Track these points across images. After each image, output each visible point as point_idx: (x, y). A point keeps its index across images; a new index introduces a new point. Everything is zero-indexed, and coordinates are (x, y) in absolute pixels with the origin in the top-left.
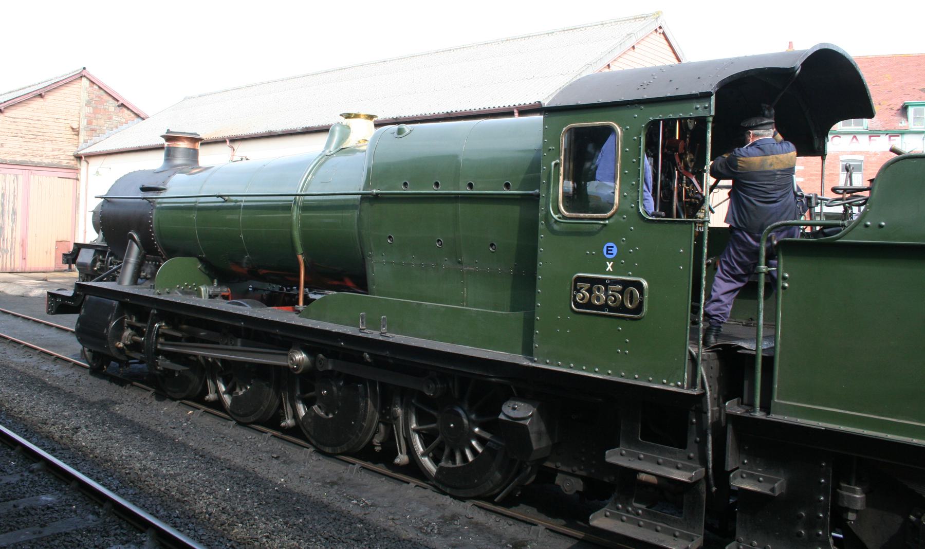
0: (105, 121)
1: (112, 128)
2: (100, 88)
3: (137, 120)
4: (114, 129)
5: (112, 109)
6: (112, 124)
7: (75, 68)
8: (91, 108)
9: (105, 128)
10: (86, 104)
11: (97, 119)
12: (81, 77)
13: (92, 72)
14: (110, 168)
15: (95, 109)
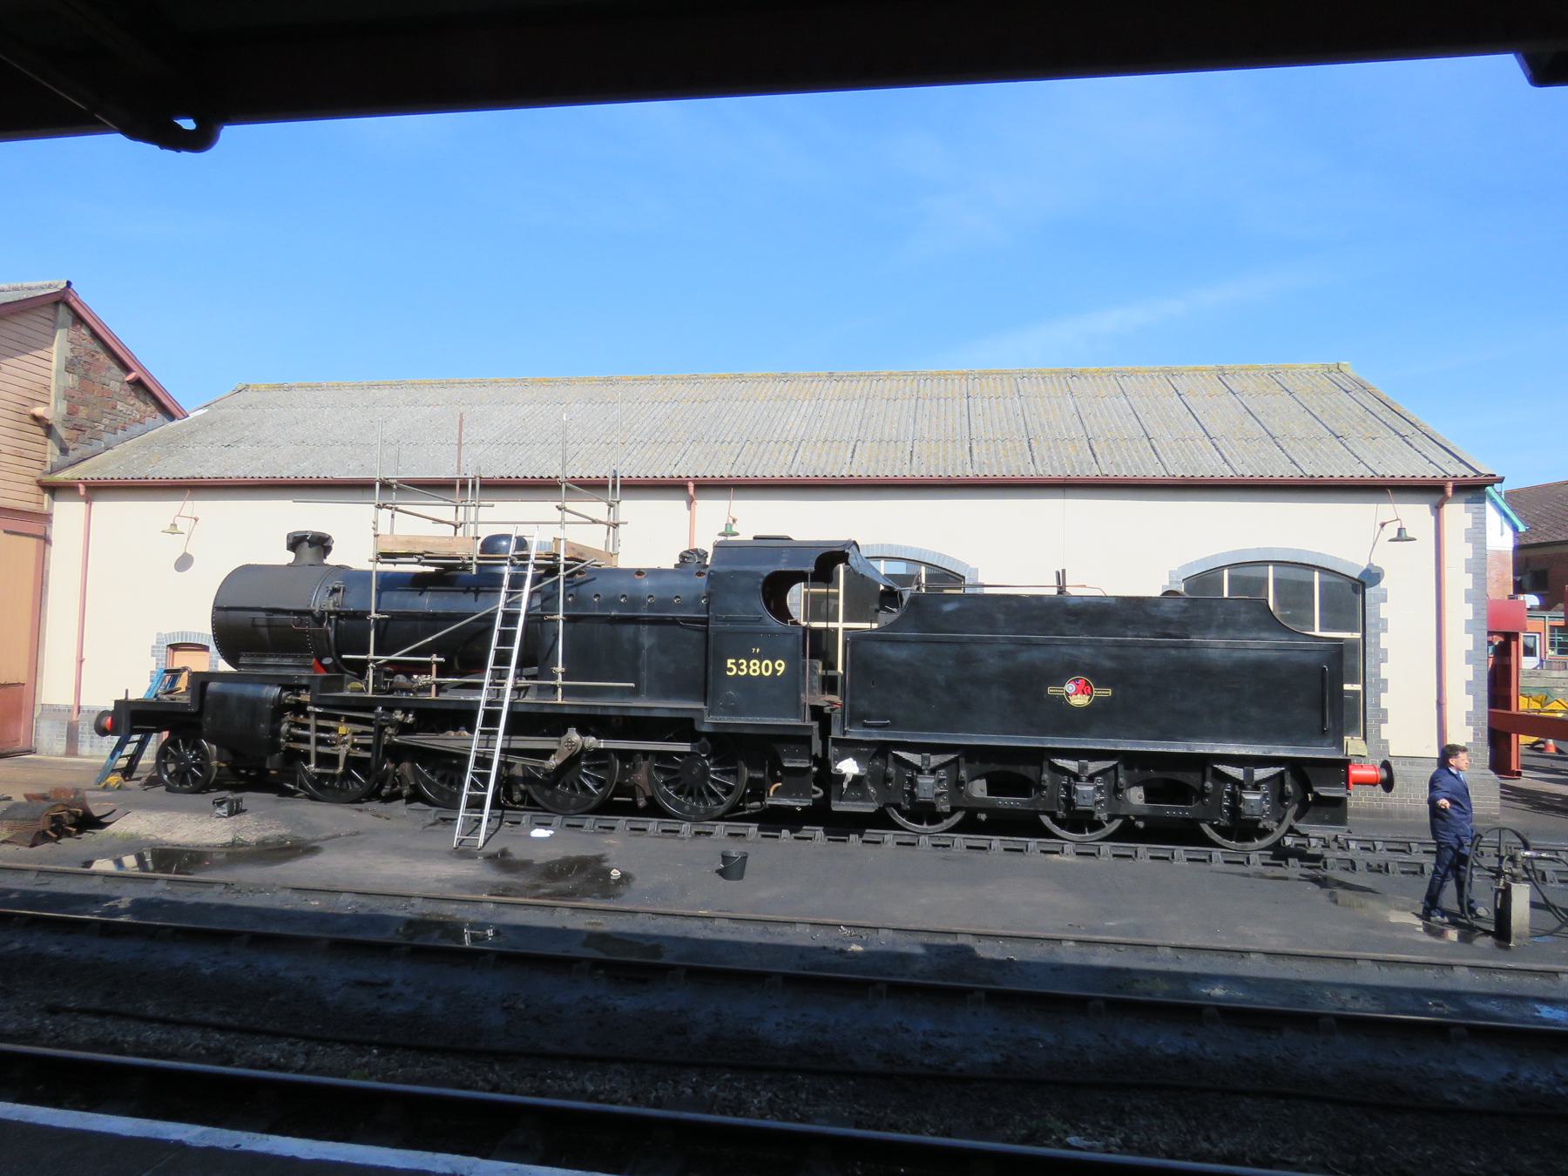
0: (103, 412)
1: (116, 429)
2: (95, 335)
3: (159, 416)
4: (119, 432)
5: (115, 386)
6: (115, 420)
7: (45, 282)
8: (76, 377)
9: (102, 427)
10: (66, 368)
11: (85, 404)
12: (56, 303)
13: (89, 297)
14: (196, 520)
15: (84, 378)
